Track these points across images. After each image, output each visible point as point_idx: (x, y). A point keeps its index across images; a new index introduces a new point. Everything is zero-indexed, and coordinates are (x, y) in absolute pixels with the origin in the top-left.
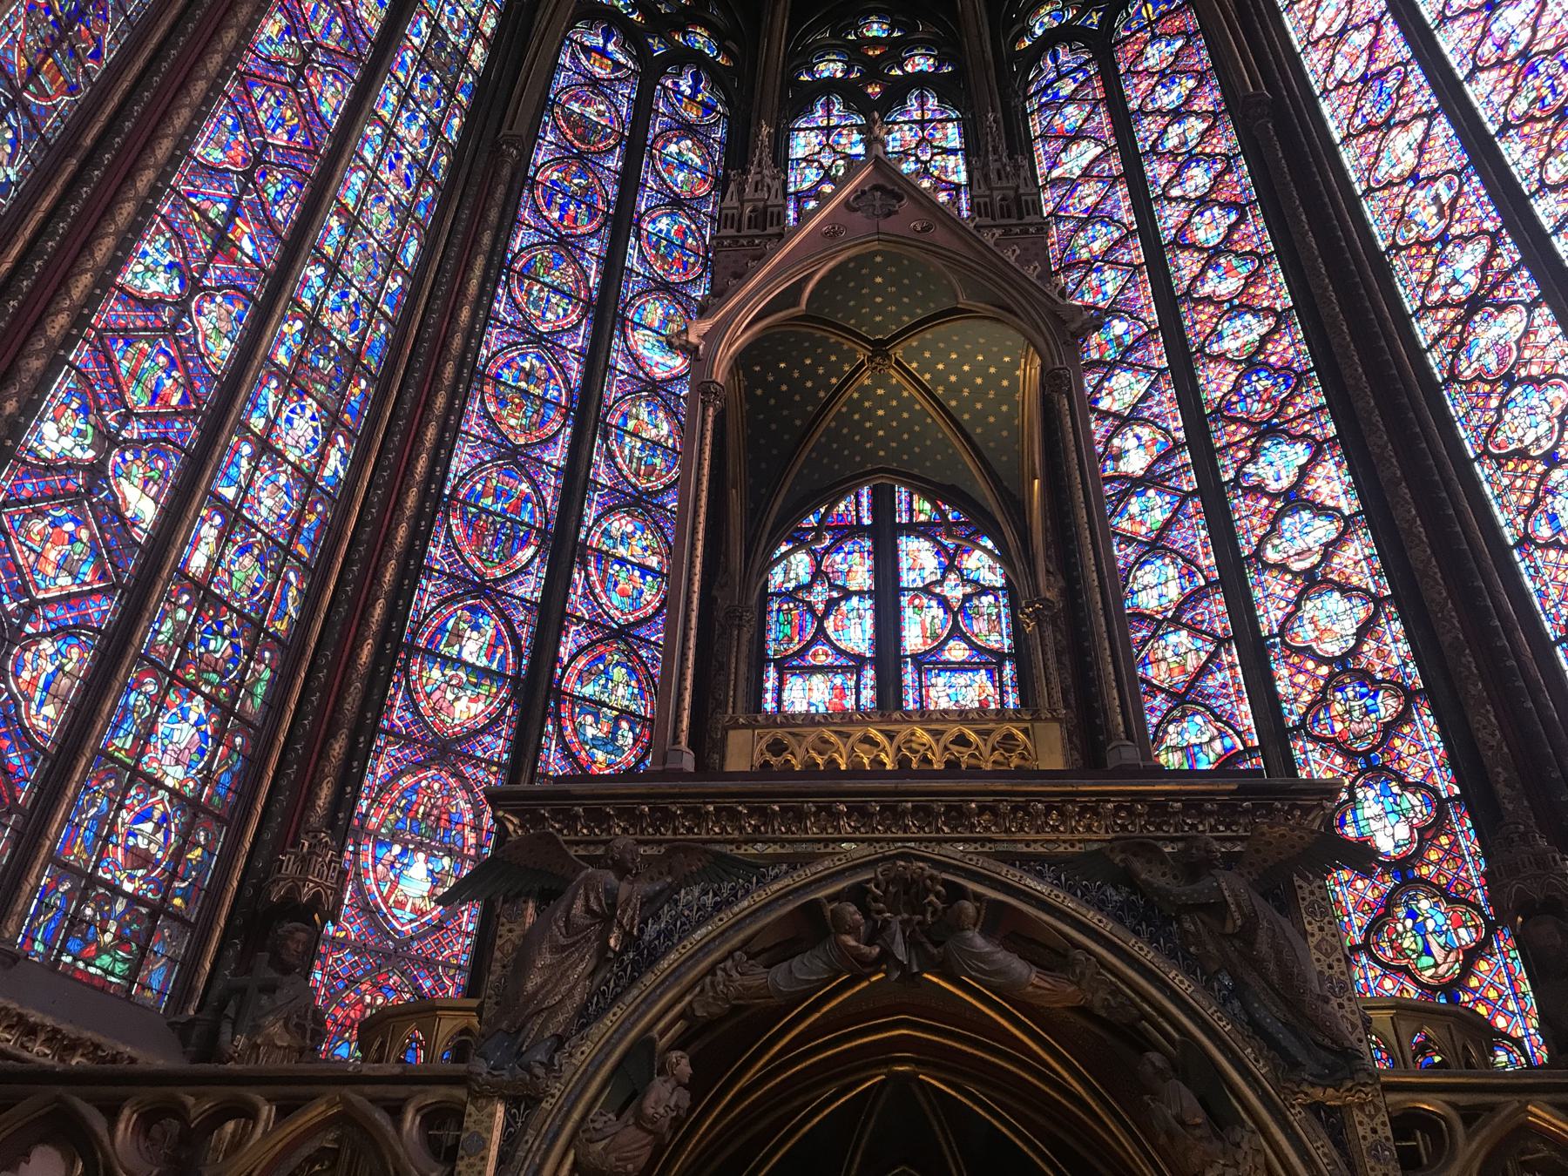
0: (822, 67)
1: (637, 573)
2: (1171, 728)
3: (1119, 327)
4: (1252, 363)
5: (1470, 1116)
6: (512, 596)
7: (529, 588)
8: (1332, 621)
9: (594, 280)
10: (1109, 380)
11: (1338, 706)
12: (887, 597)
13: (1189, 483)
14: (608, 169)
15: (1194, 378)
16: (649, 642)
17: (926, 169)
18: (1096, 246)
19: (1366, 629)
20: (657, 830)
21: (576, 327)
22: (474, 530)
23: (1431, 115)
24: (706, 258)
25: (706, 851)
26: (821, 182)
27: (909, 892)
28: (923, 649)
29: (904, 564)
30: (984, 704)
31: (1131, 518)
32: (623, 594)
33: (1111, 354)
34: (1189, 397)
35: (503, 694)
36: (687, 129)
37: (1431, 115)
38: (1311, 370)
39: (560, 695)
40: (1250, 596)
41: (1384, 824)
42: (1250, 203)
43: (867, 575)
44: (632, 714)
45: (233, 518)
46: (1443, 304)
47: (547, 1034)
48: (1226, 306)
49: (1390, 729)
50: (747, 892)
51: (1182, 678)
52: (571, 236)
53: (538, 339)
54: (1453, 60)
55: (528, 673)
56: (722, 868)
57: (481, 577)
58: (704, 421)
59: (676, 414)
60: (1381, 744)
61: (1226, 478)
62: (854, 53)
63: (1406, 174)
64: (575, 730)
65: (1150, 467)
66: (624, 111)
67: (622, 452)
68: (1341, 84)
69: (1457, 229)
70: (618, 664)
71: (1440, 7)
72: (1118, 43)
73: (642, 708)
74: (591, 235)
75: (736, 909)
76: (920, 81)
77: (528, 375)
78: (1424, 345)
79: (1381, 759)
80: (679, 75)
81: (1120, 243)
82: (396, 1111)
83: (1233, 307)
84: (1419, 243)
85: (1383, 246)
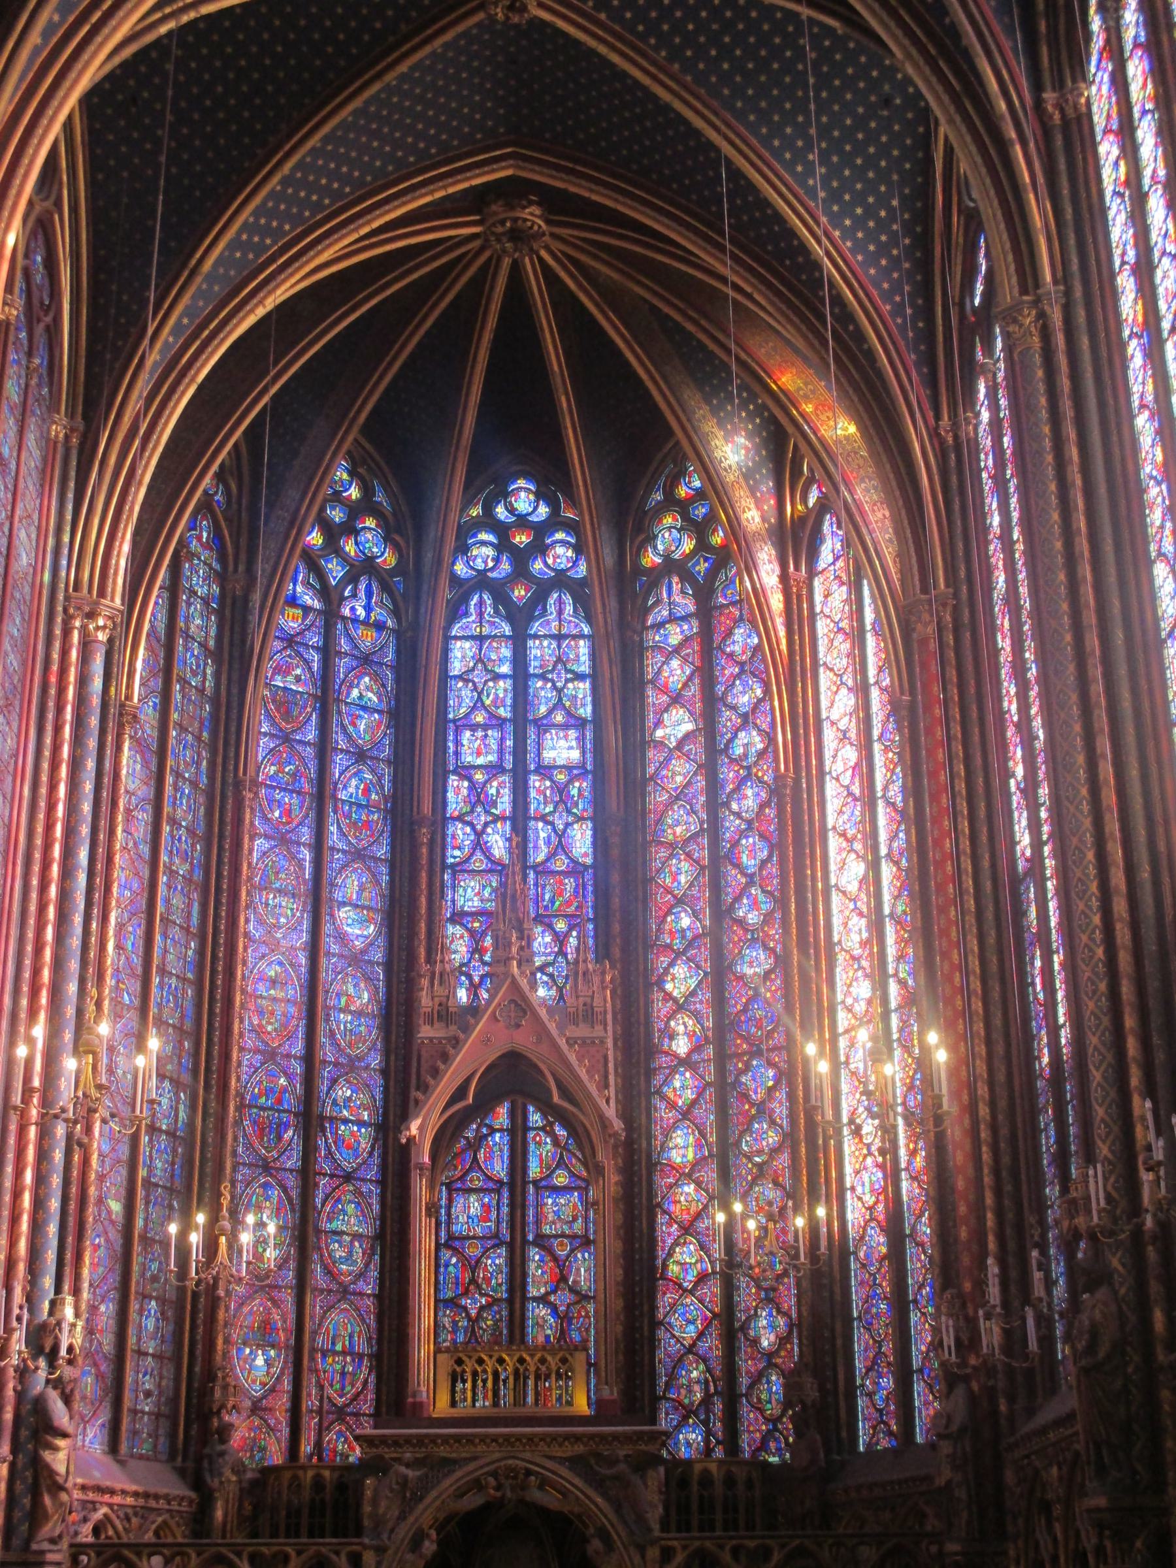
3: (685, 921)
5: (685, 1547)
6: (285, 1170)
7: (293, 1161)
17: (560, 699)
18: (678, 830)
21: (300, 923)
24: (385, 810)
26: (474, 708)
32: (349, 1147)
33: (677, 944)
36: (366, 661)
39: (318, 1231)
41: (766, 1331)
57: (265, 1159)
65: (689, 1054)
69: (864, 963)
70: (350, 1202)
76: (561, 580)
77: (273, 982)
78: (841, 1030)
79: (772, 1295)
80: (354, 595)
81: (695, 836)
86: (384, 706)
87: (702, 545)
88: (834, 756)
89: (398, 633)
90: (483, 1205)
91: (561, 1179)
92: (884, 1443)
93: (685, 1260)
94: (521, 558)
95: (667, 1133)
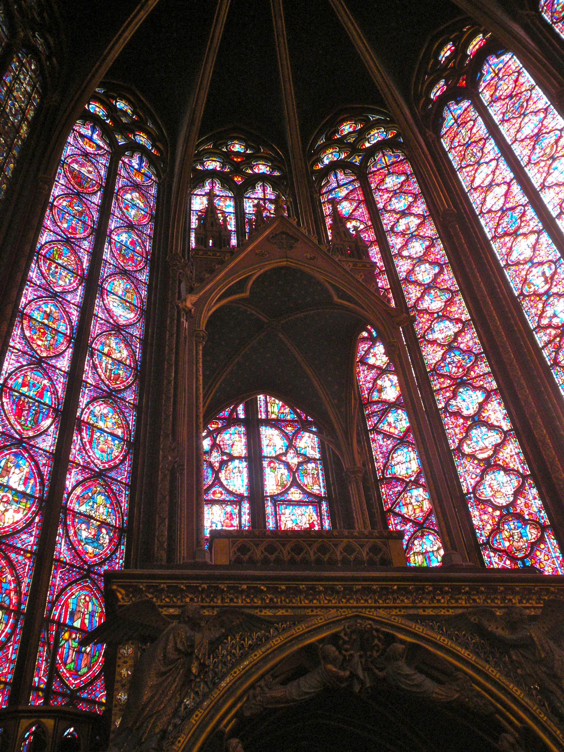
0: (208, 163)
1: (110, 438)
2: (416, 542)
4: (451, 346)
7: (47, 443)
8: (500, 487)
9: (85, 265)
10: (373, 348)
11: (506, 532)
12: (255, 459)
14: (94, 203)
15: (420, 352)
16: (117, 480)
19: (518, 492)
20: (212, 600)
22: (17, 406)
23: (539, 232)
24: (146, 258)
25: (243, 613)
28: (277, 492)
29: (265, 442)
30: (312, 525)
31: (390, 424)
32: (103, 451)
35: (33, 509)
36: (136, 187)
37: (539, 232)
38: (482, 353)
39: (67, 510)
40: (456, 471)
42: (445, 263)
43: (243, 447)
44: (108, 524)
46: (549, 326)
47: (157, 730)
48: (436, 315)
50: (268, 639)
51: (421, 514)
52: (73, 238)
53: (54, 296)
54: (550, 207)
55: (49, 496)
58: (197, 353)
59: (131, 345)
60: (530, 553)
61: (440, 406)
62: (227, 158)
63: (527, 260)
64: (75, 533)
66: (103, 173)
67: (101, 365)
68: (490, 211)
69: (555, 290)
70: (100, 493)
71: (542, 181)
72: (370, 173)
74: (85, 239)
75: (263, 649)
77: (48, 315)
78: (540, 346)
80: (132, 157)
83: (439, 317)
84: (535, 294)
85: (516, 294)
86: (148, 210)
88: (483, 202)
89: (159, 185)
90: (226, 513)
94: (237, 169)
95: (388, 456)
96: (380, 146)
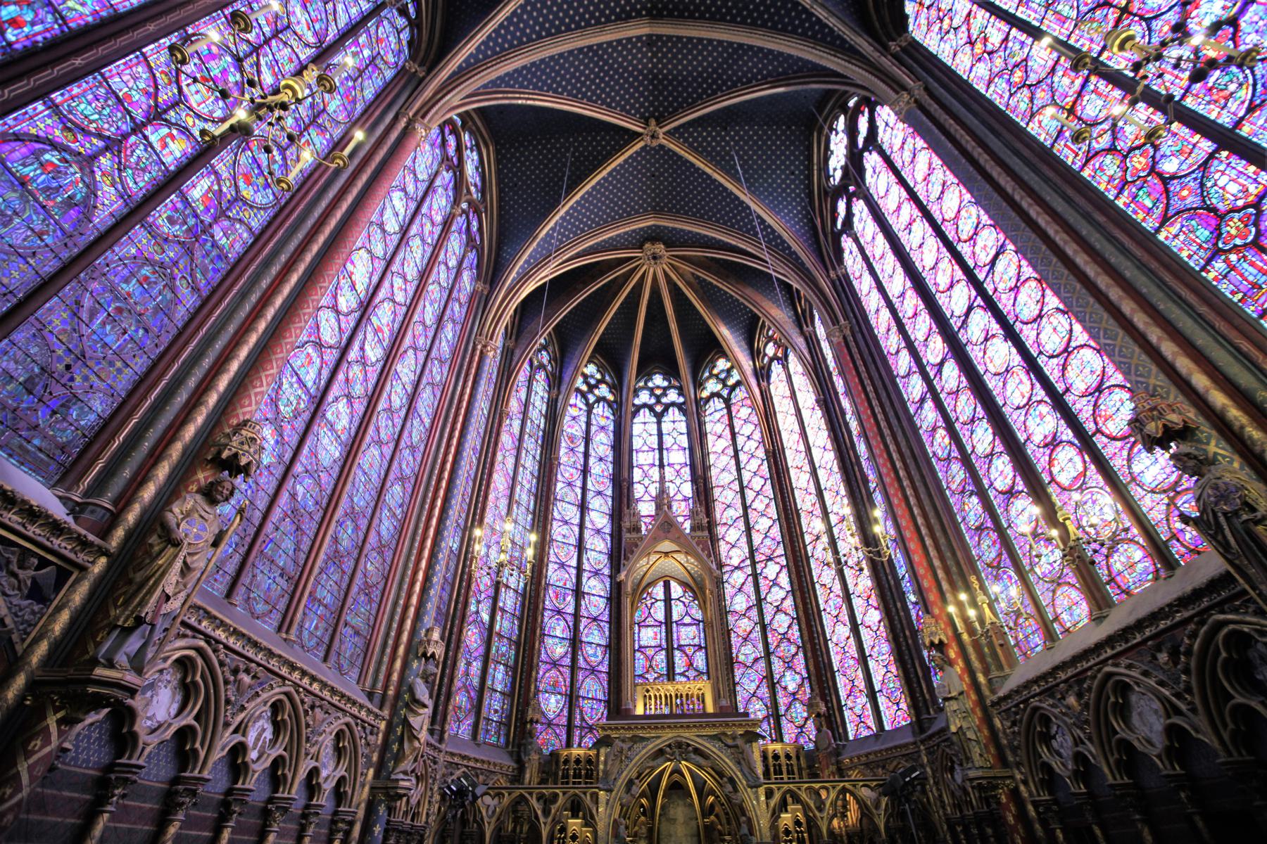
7: (571, 609)
12: (668, 600)
13: (749, 570)
27: (679, 745)
33: (730, 522)
34: (750, 542)
39: (581, 642)
41: (791, 682)
45: (503, 610)
49: (793, 656)
53: (566, 523)
56: (643, 739)
62: (652, 390)
73: (603, 643)
76: (673, 404)
82: (585, 793)
87: (725, 385)
91: (687, 620)
92: (865, 733)
93: (747, 653)
94: (658, 398)
96: (738, 384)
